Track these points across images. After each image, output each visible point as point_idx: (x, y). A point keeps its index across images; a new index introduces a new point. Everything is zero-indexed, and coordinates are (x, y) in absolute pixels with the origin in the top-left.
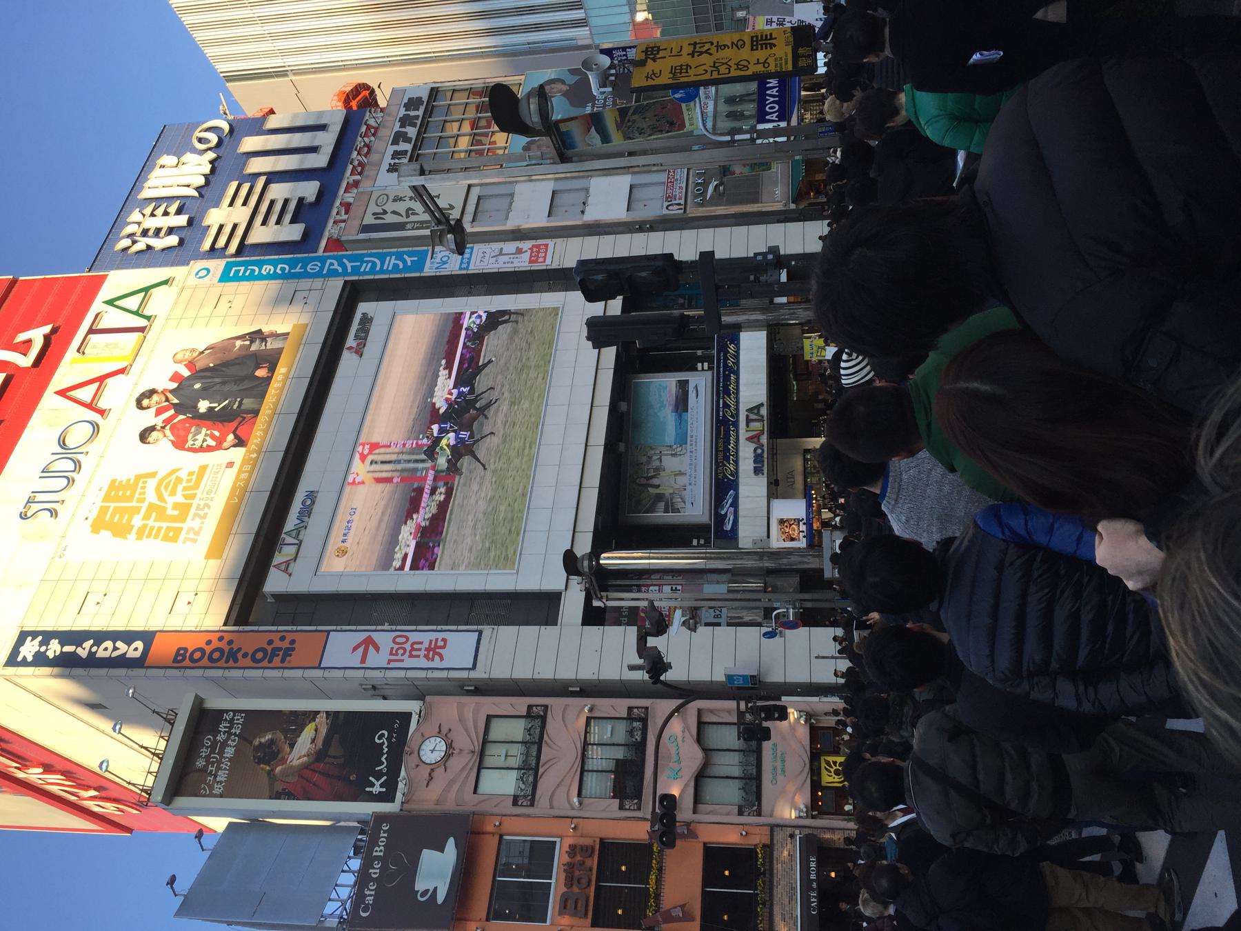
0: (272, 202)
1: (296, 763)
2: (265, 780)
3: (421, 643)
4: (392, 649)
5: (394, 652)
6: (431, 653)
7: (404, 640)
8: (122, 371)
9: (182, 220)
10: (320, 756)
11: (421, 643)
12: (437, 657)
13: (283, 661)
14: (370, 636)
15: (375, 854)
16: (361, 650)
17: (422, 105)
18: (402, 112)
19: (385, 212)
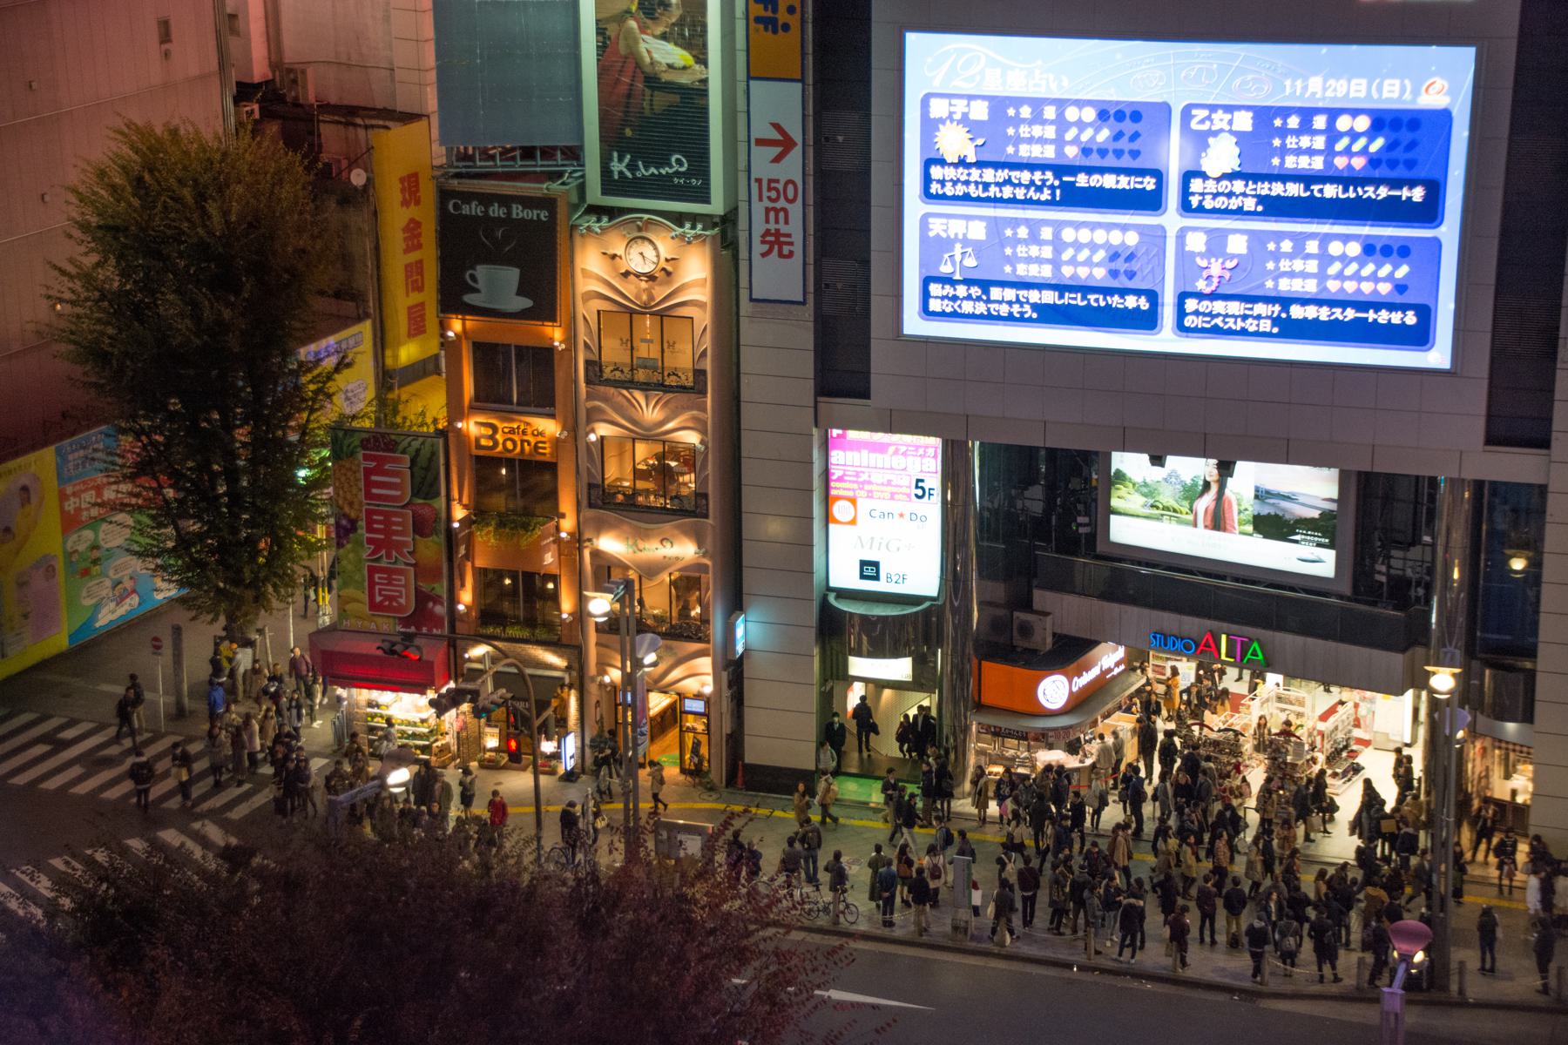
1: (642, 47)
2: (620, 6)
3: (786, 222)
4: (777, 181)
5: (773, 185)
6: (772, 239)
7: (790, 195)
10: (653, 81)
11: (786, 222)
12: (766, 247)
13: (758, 20)
14: (795, 144)
15: (514, 206)
16: (777, 136)
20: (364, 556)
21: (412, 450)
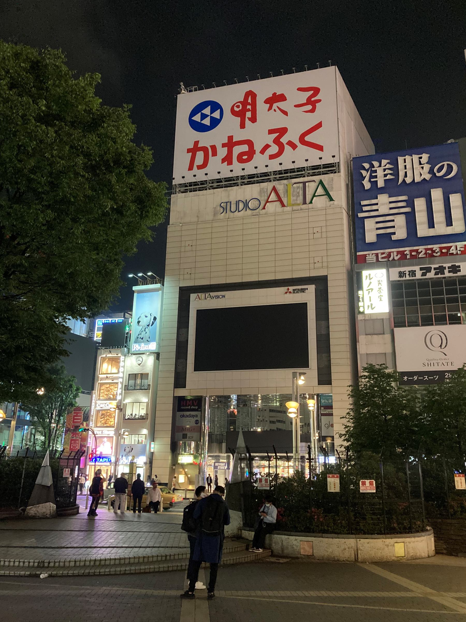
0: (393, 221)
8: (283, 205)
9: (381, 184)
17: (454, 273)
18: (446, 265)
19: (370, 279)
20: (70, 437)
21: (84, 410)
